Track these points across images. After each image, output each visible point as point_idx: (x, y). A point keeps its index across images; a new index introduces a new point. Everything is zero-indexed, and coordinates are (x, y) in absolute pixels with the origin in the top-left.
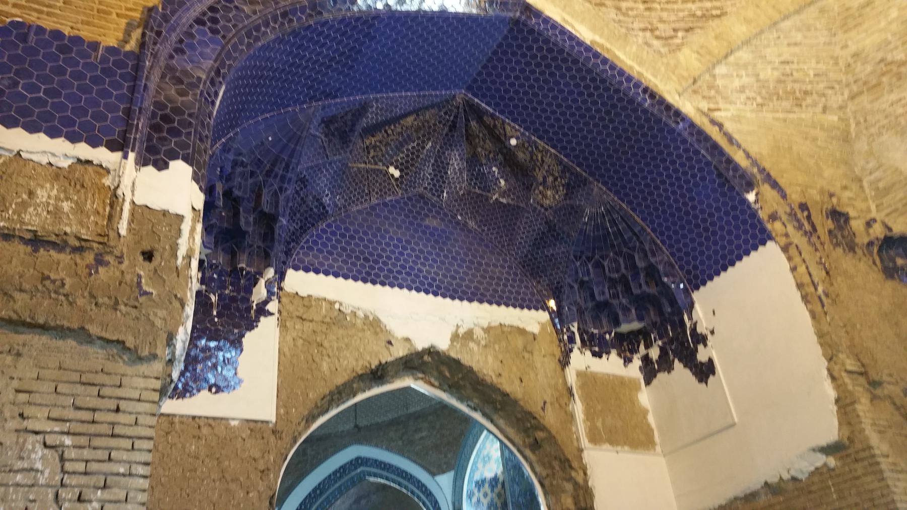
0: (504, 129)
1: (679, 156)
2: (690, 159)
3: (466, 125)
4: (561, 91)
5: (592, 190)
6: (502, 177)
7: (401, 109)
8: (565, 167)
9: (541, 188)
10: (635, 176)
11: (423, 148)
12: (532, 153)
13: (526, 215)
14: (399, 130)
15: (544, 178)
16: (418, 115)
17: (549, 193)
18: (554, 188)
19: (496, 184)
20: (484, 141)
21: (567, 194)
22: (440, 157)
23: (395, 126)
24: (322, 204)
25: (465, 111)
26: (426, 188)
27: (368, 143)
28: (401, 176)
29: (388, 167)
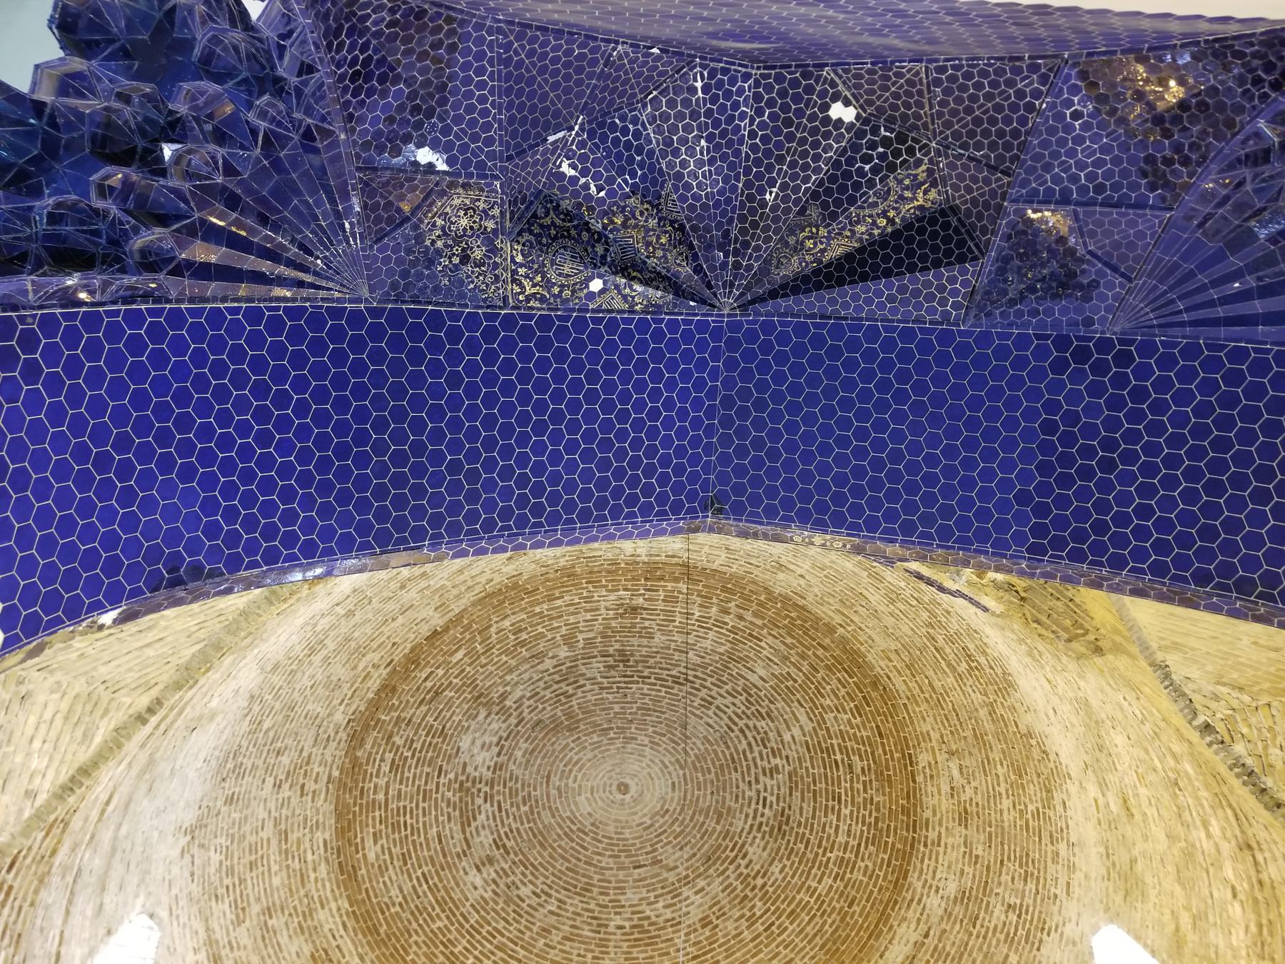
0: (625, 297)
1: (289, 517)
2: (270, 532)
3: (695, 257)
4: (572, 447)
5: (371, 291)
6: (573, 180)
7: (879, 294)
8: (462, 296)
9: (490, 225)
10: (321, 396)
11: (784, 187)
12: (548, 284)
13: (496, 147)
14: (861, 229)
15: (493, 250)
16: (820, 262)
17: (464, 222)
18: (458, 239)
19: (584, 159)
20: (648, 244)
21: (419, 239)
22: (732, 167)
23: (870, 234)
24: (1102, 99)
25: (709, 286)
26: (746, 77)
27: (933, 194)
28: (826, 107)
29: (858, 117)
